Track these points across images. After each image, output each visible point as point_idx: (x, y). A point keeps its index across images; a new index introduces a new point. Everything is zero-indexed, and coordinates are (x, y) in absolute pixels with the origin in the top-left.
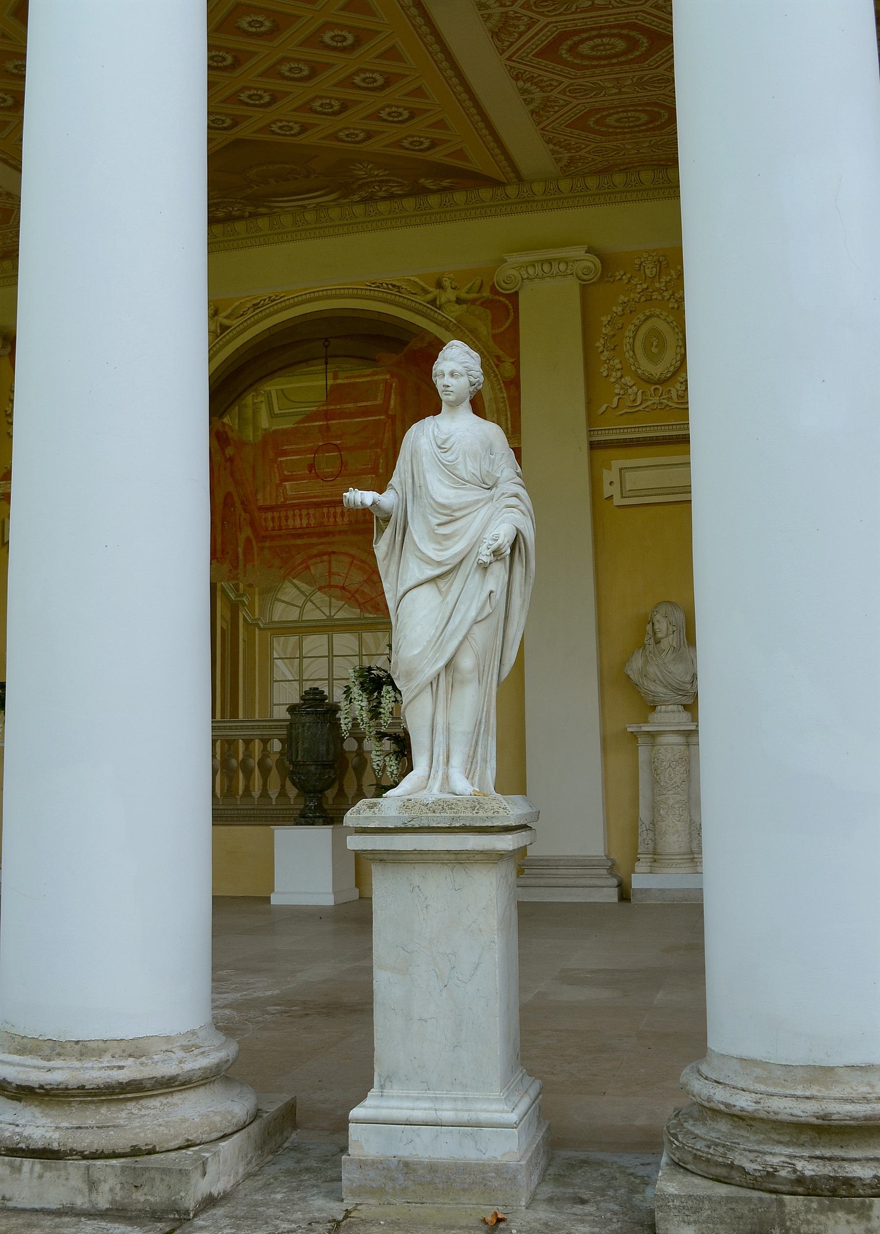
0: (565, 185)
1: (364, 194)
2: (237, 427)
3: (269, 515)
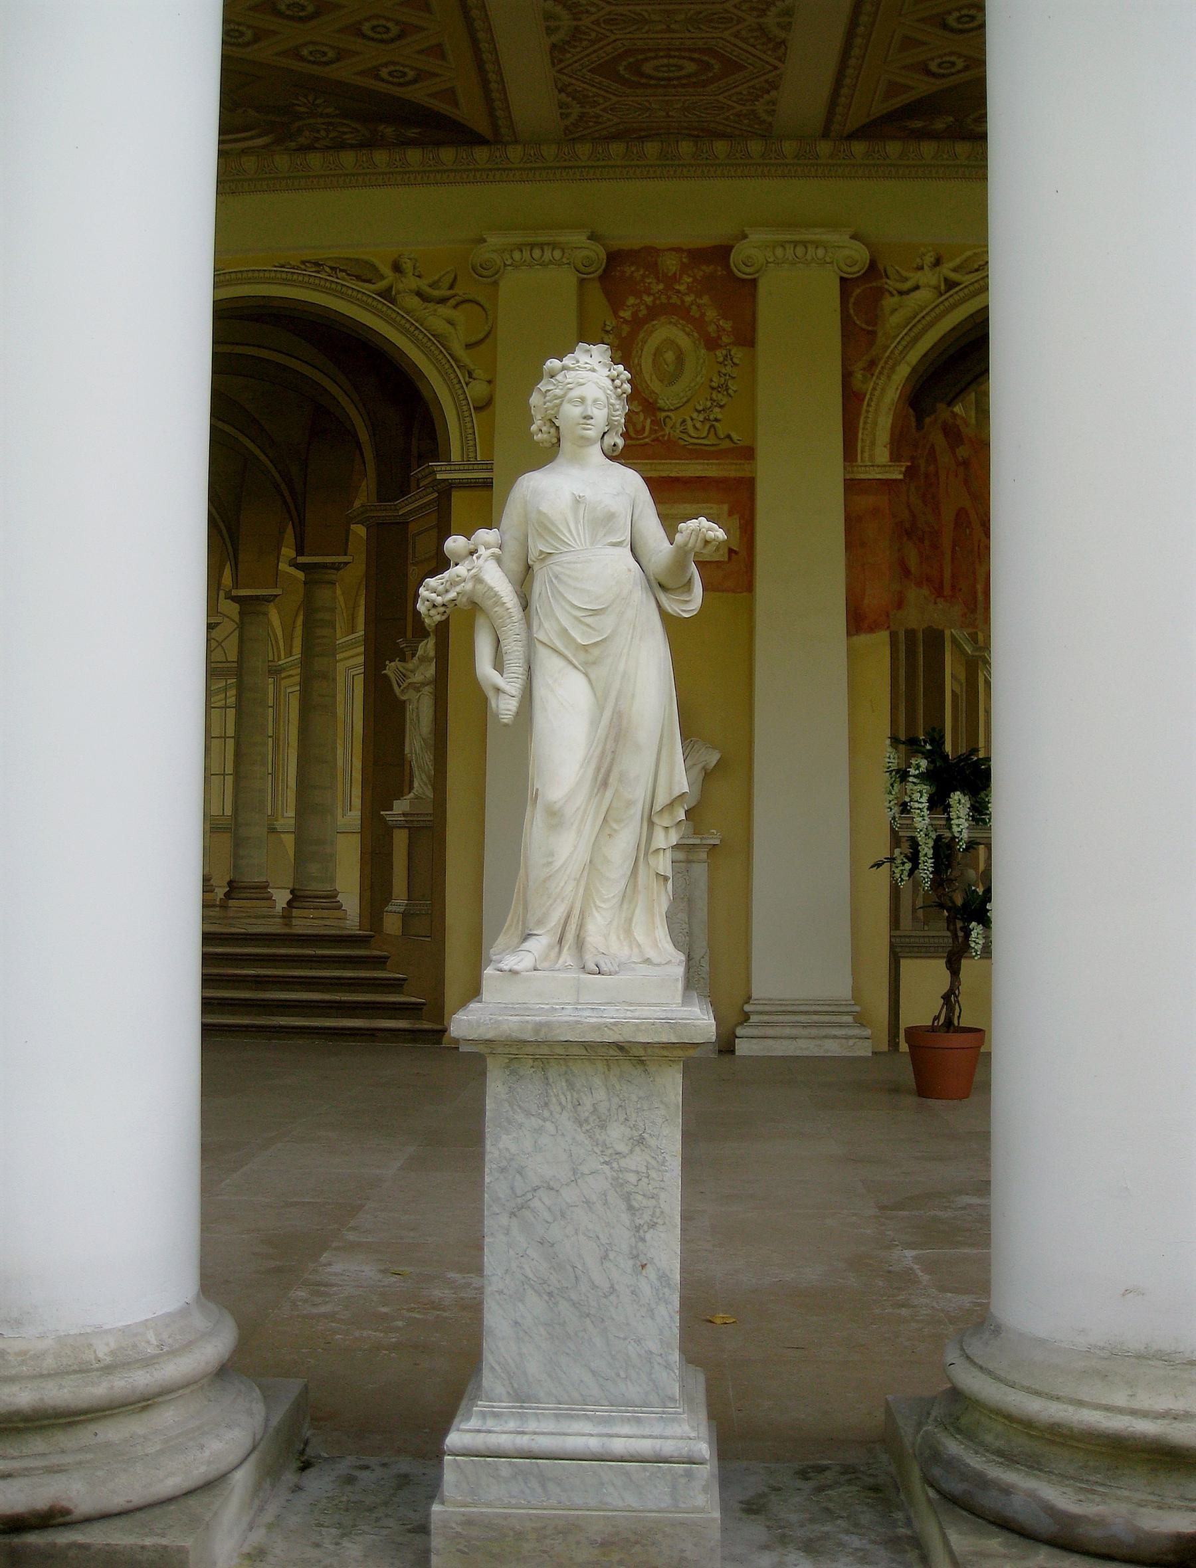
2: (973, 421)
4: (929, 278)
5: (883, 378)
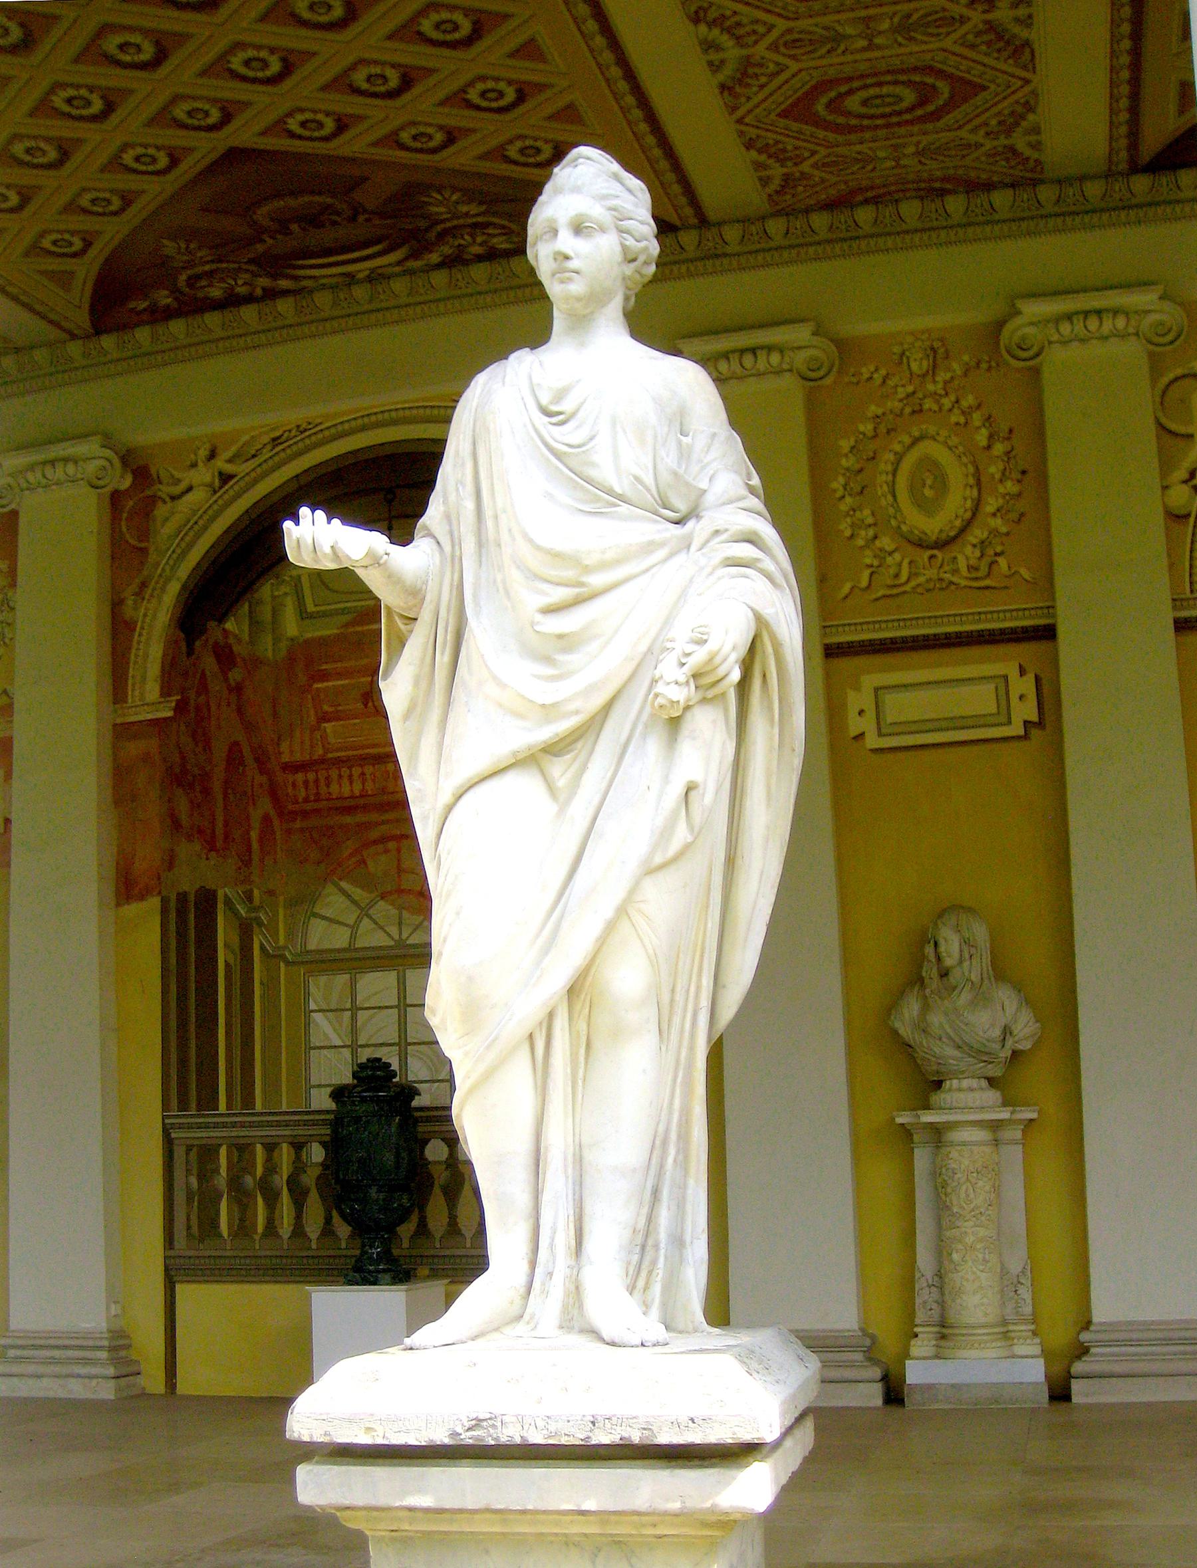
0: (775, 227)
1: (447, 250)
3: (300, 777)
4: (204, 475)
5: (154, 601)
